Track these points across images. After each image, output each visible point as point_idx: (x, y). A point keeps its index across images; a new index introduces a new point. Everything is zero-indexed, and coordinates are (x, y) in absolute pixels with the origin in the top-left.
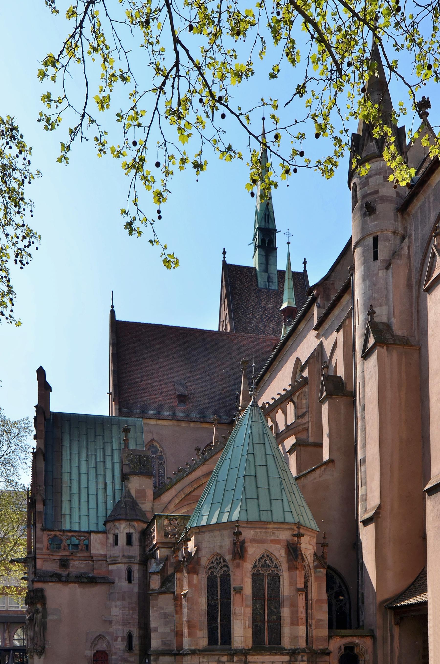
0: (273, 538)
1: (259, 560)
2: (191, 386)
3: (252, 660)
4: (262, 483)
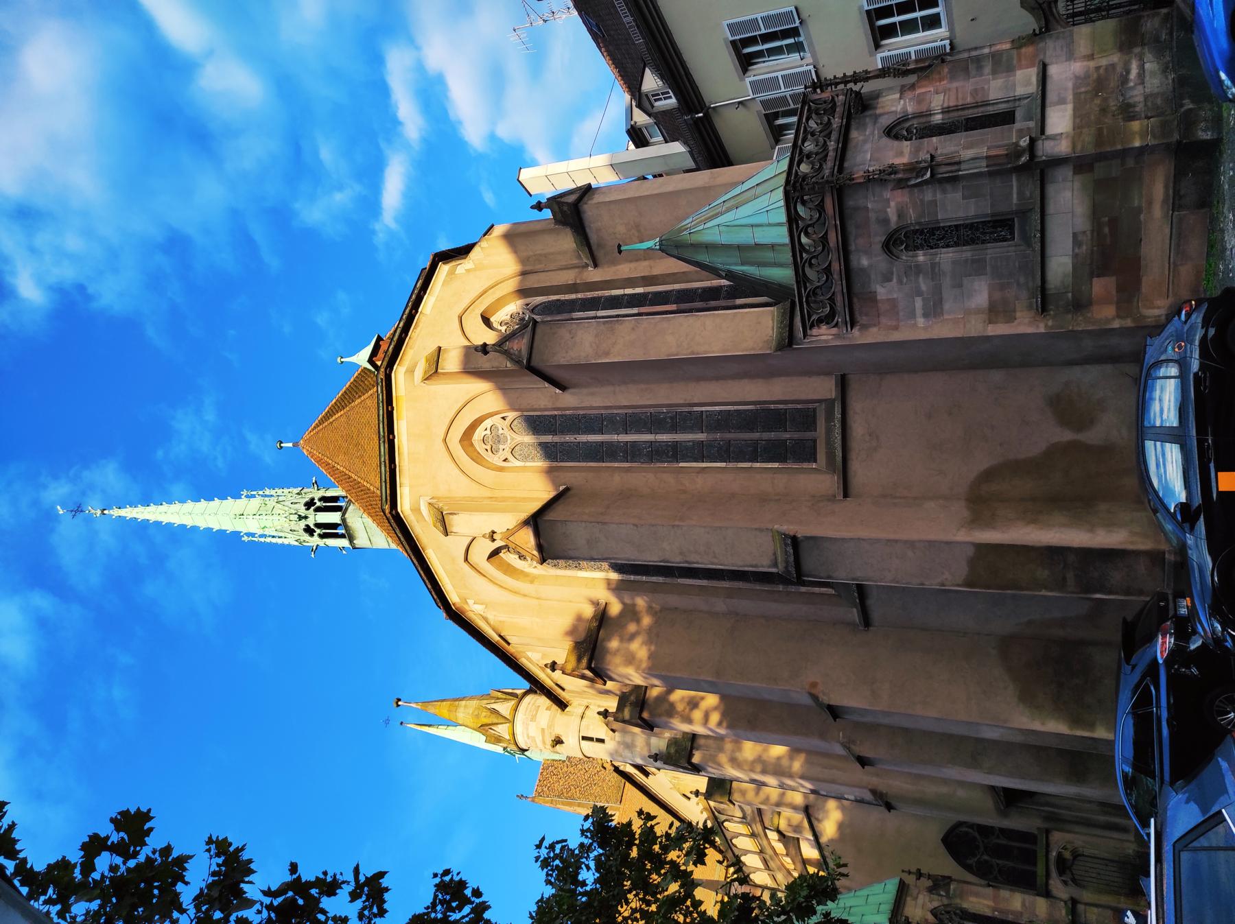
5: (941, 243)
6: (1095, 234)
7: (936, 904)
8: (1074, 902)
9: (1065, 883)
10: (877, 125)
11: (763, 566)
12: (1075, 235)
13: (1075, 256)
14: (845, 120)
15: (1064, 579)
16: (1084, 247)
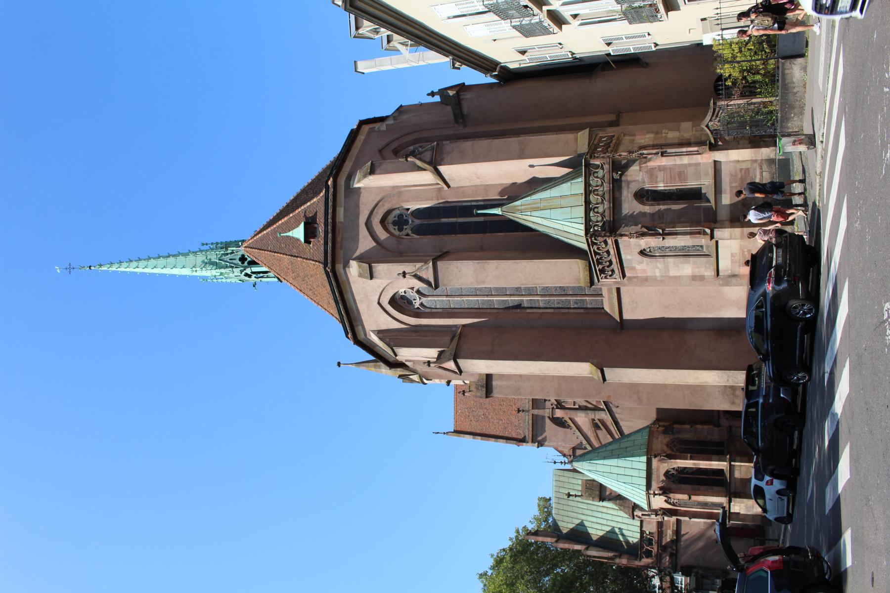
0: (656, 470)
4: (621, 471)
5: (668, 250)
6: (741, 254)
7: (667, 439)
8: (730, 427)
9: (727, 419)
10: (630, 190)
12: (732, 254)
13: (732, 260)
14: (611, 185)
15: (728, 380)
16: (736, 258)
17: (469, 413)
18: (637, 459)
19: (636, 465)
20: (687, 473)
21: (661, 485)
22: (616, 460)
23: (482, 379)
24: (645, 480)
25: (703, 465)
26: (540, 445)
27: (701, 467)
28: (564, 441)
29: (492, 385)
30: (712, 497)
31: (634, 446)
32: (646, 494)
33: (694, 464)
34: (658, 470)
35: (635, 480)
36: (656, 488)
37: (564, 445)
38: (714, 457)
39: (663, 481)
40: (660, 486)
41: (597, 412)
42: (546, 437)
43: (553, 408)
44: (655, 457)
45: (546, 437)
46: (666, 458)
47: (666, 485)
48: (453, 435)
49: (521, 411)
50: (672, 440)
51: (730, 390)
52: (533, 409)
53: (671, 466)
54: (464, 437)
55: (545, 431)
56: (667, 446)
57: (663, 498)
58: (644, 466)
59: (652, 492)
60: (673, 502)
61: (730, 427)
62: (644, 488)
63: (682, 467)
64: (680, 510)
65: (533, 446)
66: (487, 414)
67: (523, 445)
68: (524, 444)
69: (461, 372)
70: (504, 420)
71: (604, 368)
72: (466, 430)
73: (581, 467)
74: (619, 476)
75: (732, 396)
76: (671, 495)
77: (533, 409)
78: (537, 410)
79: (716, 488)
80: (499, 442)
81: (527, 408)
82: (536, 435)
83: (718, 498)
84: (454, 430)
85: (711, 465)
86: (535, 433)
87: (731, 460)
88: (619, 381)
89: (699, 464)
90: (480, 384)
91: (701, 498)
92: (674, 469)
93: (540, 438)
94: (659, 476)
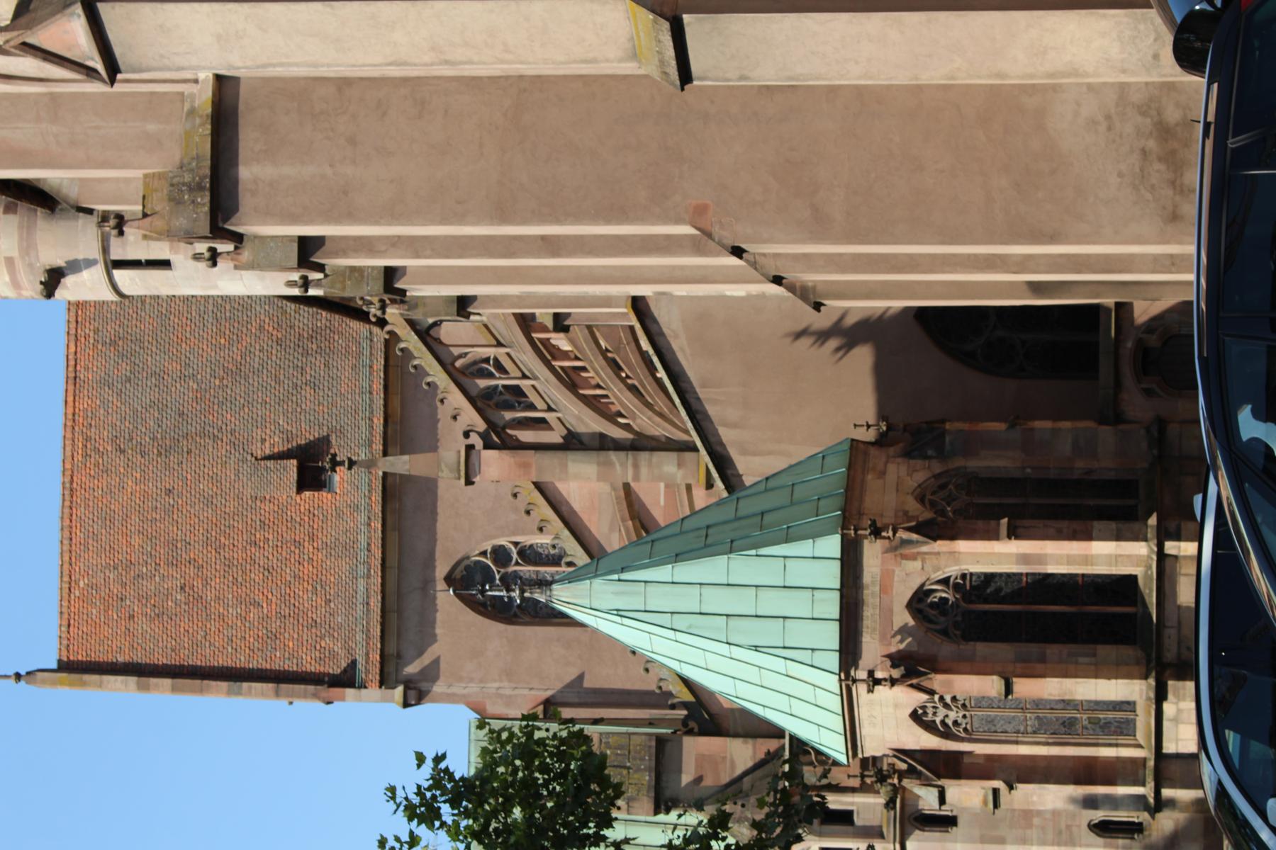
1: (930, 621)
2: (263, 441)
3: (1174, 649)
7: (920, 477)
8: (1161, 423)
9: (1148, 393)
11: (607, 61)
15: (1156, 57)
17: (124, 585)
18: (803, 548)
19: (801, 573)
20: (997, 597)
21: (896, 646)
22: (723, 559)
23: (198, 158)
24: (835, 627)
25: (1058, 560)
26: (412, 693)
27: (1051, 569)
28: (509, 674)
29: (235, 182)
30: (1093, 681)
31: (792, 504)
32: (840, 680)
33: (1025, 559)
34: (885, 588)
35: (801, 634)
36: (879, 660)
37: (508, 692)
38: (1098, 525)
39: (904, 631)
40: (893, 649)
41: (644, 456)
42: (436, 662)
43: (470, 448)
44: (876, 532)
45: (436, 662)
46: (915, 536)
47: (915, 648)
48: (54, 683)
49: (342, 463)
50: (936, 477)
51: (1162, 167)
52: (385, 454)
53: (937, 569)
54: (100, 686)
55: (433, 638)
56: (921, 499)
57: (907, 698)
58: (831, 575)
59: (862, 674)
60: (943, 722)
61: (1161, 423)
62: (833, 661)
63: (979, 575)
64: (970, 753)
65: (384, 700)
66: (198, 583)
67: (343, 699)
68: (350, 692)
69: (113, 68)
70: (269, 603)
71: (685, 16)
72: (109, 658)
73: (586, 602)
74: (733, 621)
75: (1170, 192)
76: (937, 681)
77: (385, 454)
78: (406, 458)
79: (1104, 651)
80: (249, 694)
81: (362, 456)
82: (399, 656)
83: (1113, 681)
84: (60, 661)
85: (1087, 559)
86: (392, 648)
87: (1164, 534)
88: (742, 78)
89: (1041, 559)
90: (187, 178)
91: (1052, 688)
92: (945, 581)
93: (412, 669)
94: (891, 611)
